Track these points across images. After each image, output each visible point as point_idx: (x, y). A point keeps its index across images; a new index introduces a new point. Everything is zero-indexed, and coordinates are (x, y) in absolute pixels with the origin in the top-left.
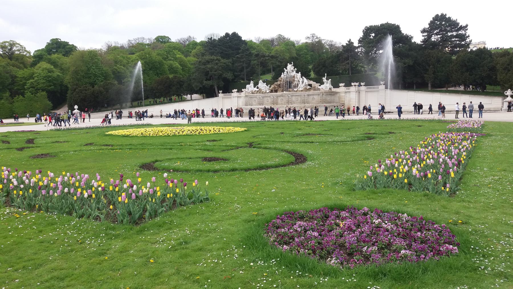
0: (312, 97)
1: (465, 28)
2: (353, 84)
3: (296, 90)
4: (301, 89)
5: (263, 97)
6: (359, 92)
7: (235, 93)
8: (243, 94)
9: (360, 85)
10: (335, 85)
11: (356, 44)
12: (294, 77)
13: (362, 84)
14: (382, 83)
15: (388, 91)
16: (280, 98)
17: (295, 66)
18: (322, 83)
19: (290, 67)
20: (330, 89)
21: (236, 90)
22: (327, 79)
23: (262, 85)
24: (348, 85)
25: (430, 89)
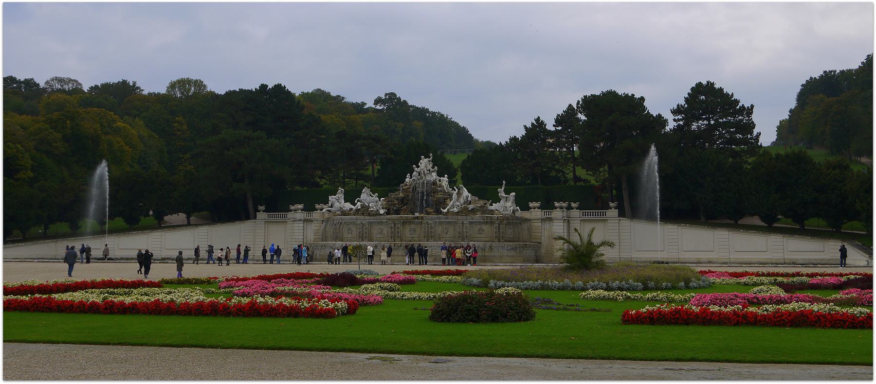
0: (478, 227)
1: (750, 111)
2: (557, 204)
3: (445, 211)
4: (455, 210)
5: (370, 223)
6: (568, 221)
7: (297, 212)
8: (316, 215)
9: (569, 208)
10: (522, 203)
11: (550, 127)
12: (434, 183)
13: (573, 205)
14: (611, 204)
15: (626, 223)
16: (408, 228)
17: (435, 163)
18: (497, 200)
19: (425, 163)
20: (514, 212)
21: (301, 206)
22: (507, 192)
23: (367, 197)
24: (547, 206)
25: (703, 219)
